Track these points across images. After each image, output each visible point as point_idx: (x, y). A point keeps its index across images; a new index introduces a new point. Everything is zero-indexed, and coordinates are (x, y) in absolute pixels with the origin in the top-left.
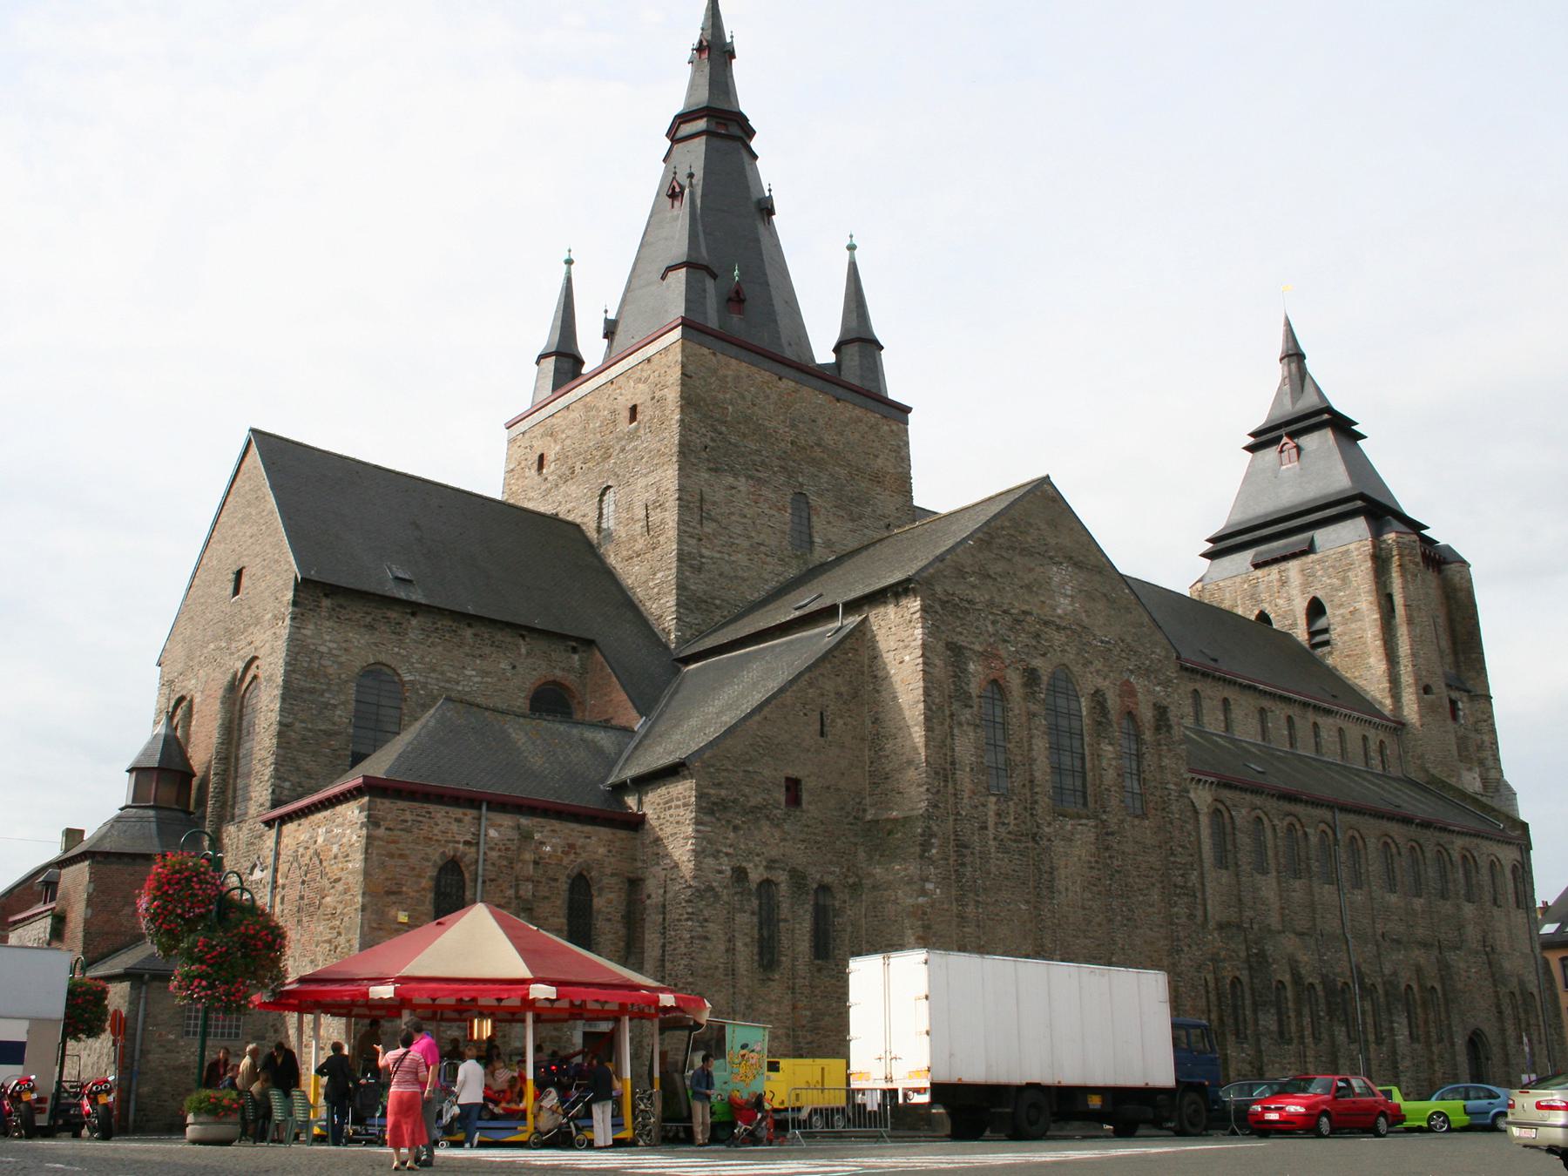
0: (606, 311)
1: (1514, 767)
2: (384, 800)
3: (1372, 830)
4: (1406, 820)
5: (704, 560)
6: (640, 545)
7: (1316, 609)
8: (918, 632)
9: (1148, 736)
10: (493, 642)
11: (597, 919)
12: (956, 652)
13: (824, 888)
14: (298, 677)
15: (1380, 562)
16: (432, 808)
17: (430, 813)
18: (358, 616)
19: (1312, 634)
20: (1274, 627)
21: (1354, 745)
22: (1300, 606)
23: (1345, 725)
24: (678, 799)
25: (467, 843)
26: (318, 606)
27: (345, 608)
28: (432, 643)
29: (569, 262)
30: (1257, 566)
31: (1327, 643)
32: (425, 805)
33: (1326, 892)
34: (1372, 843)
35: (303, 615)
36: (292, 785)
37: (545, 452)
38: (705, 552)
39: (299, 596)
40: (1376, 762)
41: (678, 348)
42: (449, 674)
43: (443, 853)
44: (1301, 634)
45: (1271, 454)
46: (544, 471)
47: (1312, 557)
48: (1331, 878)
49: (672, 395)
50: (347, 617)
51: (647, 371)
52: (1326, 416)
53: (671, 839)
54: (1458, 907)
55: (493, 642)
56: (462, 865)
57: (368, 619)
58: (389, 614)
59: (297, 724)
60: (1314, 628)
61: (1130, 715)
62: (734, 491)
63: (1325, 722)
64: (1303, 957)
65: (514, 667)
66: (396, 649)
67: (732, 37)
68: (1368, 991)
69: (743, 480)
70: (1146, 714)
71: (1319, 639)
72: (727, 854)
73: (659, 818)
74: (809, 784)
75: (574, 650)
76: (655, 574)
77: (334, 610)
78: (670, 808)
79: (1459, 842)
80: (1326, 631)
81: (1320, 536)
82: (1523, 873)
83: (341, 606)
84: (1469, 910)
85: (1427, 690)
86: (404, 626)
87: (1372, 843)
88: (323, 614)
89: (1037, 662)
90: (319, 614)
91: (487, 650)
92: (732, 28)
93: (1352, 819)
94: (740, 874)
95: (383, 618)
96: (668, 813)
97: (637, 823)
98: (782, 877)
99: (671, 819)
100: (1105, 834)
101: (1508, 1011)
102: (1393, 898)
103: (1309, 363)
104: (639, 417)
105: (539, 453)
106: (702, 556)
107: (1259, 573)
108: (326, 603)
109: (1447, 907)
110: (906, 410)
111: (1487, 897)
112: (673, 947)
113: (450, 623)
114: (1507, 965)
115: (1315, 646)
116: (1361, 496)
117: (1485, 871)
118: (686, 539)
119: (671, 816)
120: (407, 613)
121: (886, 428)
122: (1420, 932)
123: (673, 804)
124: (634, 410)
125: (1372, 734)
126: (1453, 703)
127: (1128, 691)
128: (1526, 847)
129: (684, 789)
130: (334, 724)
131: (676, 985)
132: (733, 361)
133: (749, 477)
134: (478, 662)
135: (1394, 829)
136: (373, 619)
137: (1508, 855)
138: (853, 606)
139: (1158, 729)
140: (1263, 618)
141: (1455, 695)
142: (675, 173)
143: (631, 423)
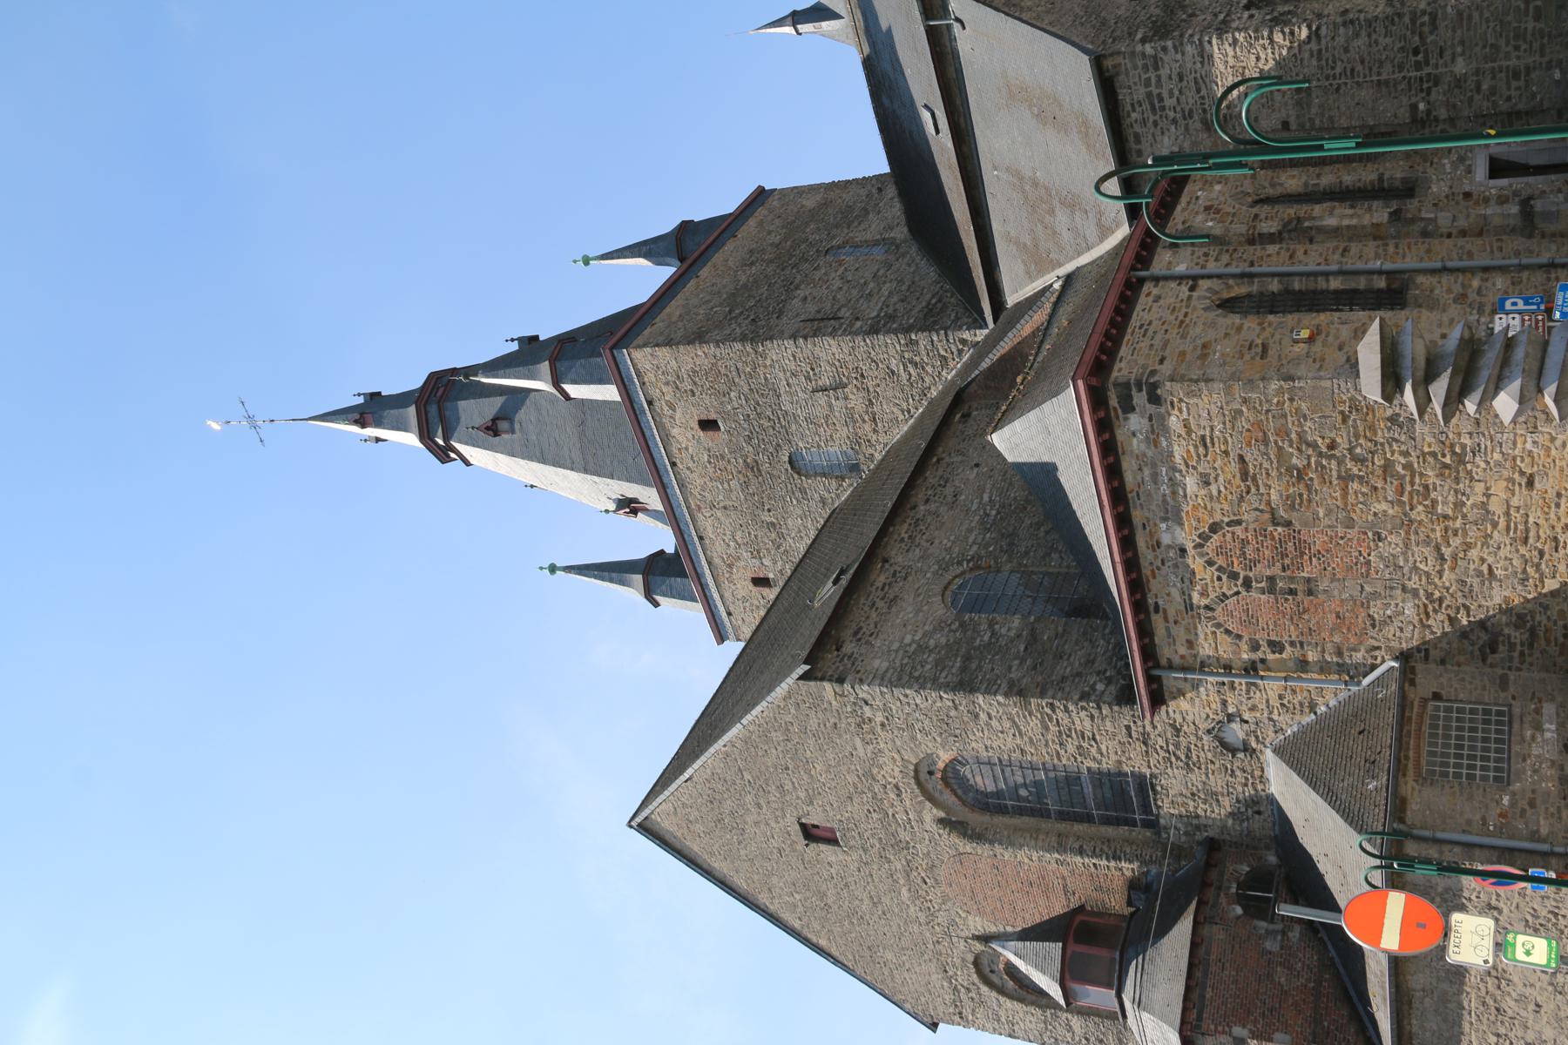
0: (607, 511)
2: (1116, 368)
5: (882, 314)
6: (857, 401)
10: (940, 485)
11: (1318, 184)
14: (943, 675)
16: (1135, 321)
17: (1142, 326)
18: (874, 615)
24: (1148, 83)
25: (1192, 289)
26: (850, 657)
27: (861, 628)
28: (927, 541)
32: (1129, 331)
35: (858, 672)
36: (1101, 681)
37: (750, 575)
38: (875, 314)
39: (831, 676)
41: (637, 354)
42: (973, 524)
43: (1205, 309)
46: (771, 576)
50: (872, 626)
53: (1204, 92)
55: (940, 485)
56: (1225, 295)
57: (880, 604)
58: (879, 584)
59: (1012, 676)
62: (809, 299)
65: (977, 465)
66: (928, 575)
67: (359, 395)
69: (799, 292)
72: (1227, 15)
73: (1174, 121)
75: (966, 416)
76: (893, 372)
77: (860, 640)
78: (1161, 100)
83: (856, 633)
86: (899, 569)
88: (863, 651)
90: (861, 655)
91: (949, 491)
95: (882, 589)
96: (1169, 102)
99: (1176, 92)
104: (713, 416)
105: (751, 586)
106: (878, 316)
108: (849, 648)
112: (1359, 68)
113: (906, 526)
118: (854, 329)
119: (1171, 94)
120: (882, 567)
121: (775, 203)
123: (1156, 92)
124: (708, 425)
130: (1019, 636)
131: (1416, 52)
132: (667, 310)
133: (797, 288)
134: (963, 497)
136: (882, 599)
142: (473, 428)
143: (719, 428)
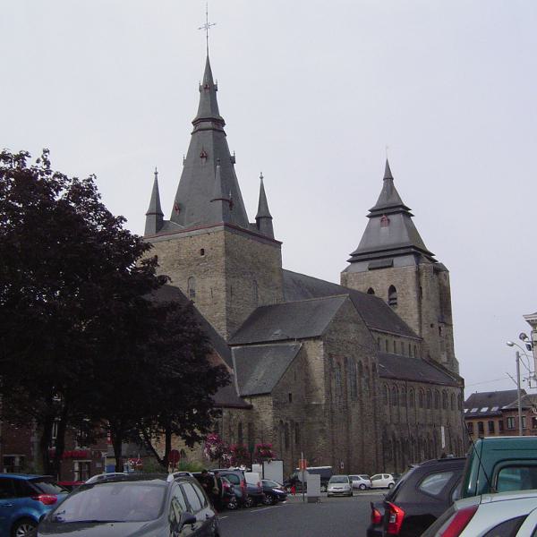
1: (459, 353)
3: (416, 385)
4: (427, 382)
7: (392, 289)
8: (322, 351)
9: (371, 373)
12: (331, 356)
13: (297, 424)
15: (418, 273)
19: (390, 300)
20: (376, 295)
21: (407, 350)
22: (387, 287)
23: (404, 341)
29: (156, 173)
30: (370, 269)
31: (396, 304)
33: (403, 409)
34: (417, 391)
40: (413, 354)
44: (386, 298)
45: (378, 220)
47: (392, 269)
48: (405, 405)
49: (221, 251)
51: (208, 237)
52: (401, 209)
54: (440, 411)
60: (391, 297)
61: (367, 367)
63: (398, 340)
64: (396, 432)
68: (414, 441)
70: (370, 366)
71: (392, 302)
74: (293, 394)
79: (443, 388)
80: (396, 299)
81: (396, 261)
82: (462, 395)
84: (444, 412)
85: (432, 326)
87: (417, 391)
89: (347, 355)
92: (217, 78)
93: (412, 383)
94: (281, 421)
97: (250, 408)
98: (288, 422)
100: (361, 404)
101: (454, 447)
102: (421, 410)
103: (395, 182)
104: (206, 254)
107: (370, 272)
109: (437, 412)
110: (280, 243)
111: (450, 407)
114: (454, 431)
115: (391, 304)
116: (414, 247)
117: (450, 398)
122: (429, 421)
125: (412, 343)
126: (440, 328)
127: (367, 360)
128: (462, 388)
129: (269, 400)
135: (421, 385)
137: (457, 391)
138: (300, 340)
139: (373, 371)
140: (371, 291)
141: (440, 325)
